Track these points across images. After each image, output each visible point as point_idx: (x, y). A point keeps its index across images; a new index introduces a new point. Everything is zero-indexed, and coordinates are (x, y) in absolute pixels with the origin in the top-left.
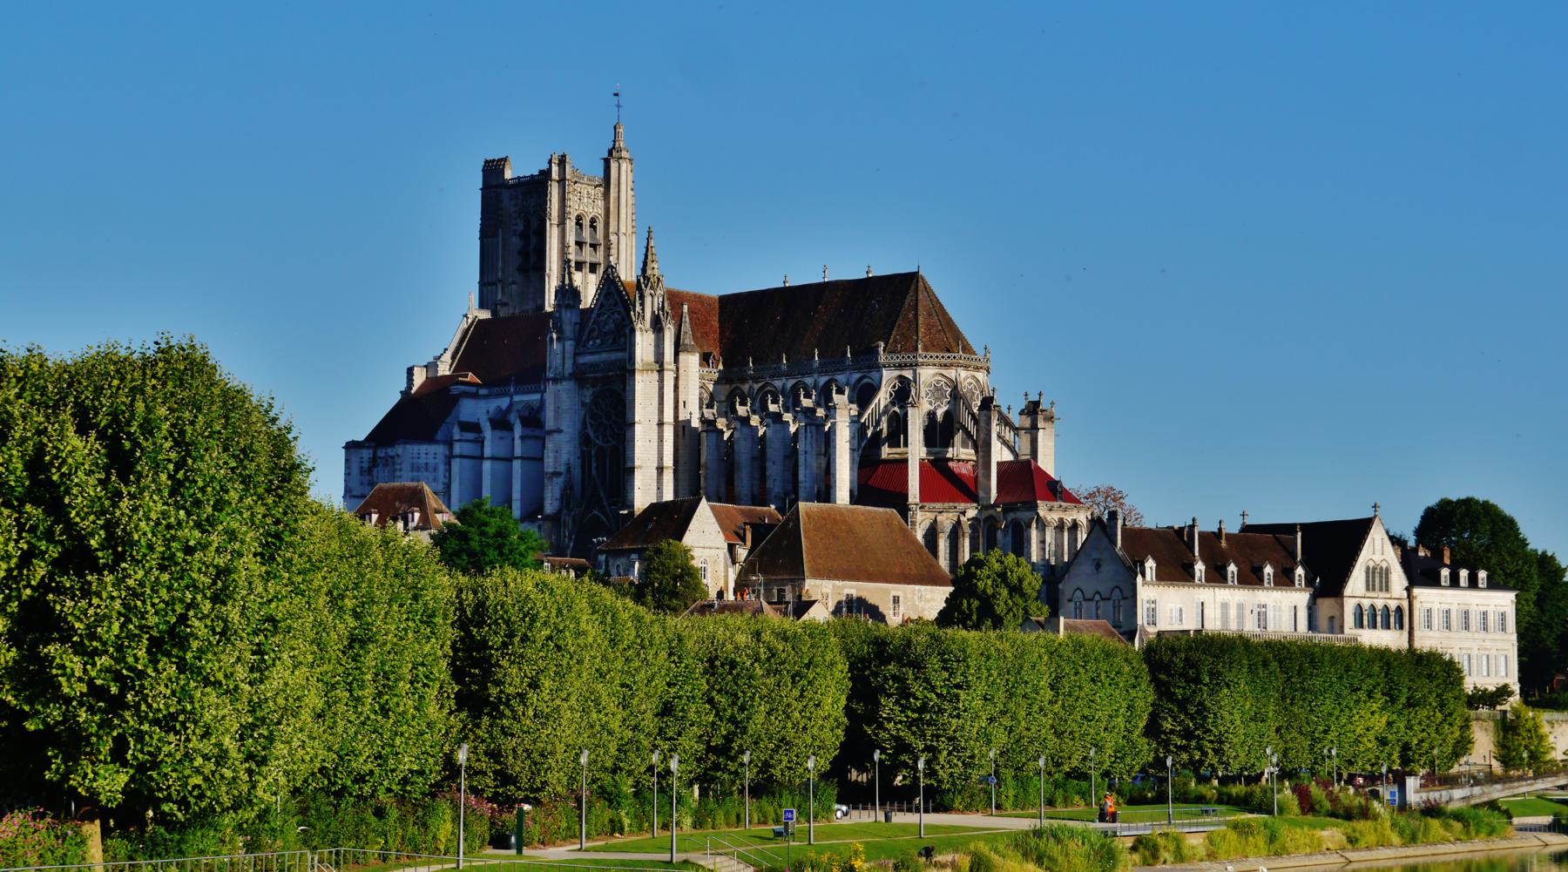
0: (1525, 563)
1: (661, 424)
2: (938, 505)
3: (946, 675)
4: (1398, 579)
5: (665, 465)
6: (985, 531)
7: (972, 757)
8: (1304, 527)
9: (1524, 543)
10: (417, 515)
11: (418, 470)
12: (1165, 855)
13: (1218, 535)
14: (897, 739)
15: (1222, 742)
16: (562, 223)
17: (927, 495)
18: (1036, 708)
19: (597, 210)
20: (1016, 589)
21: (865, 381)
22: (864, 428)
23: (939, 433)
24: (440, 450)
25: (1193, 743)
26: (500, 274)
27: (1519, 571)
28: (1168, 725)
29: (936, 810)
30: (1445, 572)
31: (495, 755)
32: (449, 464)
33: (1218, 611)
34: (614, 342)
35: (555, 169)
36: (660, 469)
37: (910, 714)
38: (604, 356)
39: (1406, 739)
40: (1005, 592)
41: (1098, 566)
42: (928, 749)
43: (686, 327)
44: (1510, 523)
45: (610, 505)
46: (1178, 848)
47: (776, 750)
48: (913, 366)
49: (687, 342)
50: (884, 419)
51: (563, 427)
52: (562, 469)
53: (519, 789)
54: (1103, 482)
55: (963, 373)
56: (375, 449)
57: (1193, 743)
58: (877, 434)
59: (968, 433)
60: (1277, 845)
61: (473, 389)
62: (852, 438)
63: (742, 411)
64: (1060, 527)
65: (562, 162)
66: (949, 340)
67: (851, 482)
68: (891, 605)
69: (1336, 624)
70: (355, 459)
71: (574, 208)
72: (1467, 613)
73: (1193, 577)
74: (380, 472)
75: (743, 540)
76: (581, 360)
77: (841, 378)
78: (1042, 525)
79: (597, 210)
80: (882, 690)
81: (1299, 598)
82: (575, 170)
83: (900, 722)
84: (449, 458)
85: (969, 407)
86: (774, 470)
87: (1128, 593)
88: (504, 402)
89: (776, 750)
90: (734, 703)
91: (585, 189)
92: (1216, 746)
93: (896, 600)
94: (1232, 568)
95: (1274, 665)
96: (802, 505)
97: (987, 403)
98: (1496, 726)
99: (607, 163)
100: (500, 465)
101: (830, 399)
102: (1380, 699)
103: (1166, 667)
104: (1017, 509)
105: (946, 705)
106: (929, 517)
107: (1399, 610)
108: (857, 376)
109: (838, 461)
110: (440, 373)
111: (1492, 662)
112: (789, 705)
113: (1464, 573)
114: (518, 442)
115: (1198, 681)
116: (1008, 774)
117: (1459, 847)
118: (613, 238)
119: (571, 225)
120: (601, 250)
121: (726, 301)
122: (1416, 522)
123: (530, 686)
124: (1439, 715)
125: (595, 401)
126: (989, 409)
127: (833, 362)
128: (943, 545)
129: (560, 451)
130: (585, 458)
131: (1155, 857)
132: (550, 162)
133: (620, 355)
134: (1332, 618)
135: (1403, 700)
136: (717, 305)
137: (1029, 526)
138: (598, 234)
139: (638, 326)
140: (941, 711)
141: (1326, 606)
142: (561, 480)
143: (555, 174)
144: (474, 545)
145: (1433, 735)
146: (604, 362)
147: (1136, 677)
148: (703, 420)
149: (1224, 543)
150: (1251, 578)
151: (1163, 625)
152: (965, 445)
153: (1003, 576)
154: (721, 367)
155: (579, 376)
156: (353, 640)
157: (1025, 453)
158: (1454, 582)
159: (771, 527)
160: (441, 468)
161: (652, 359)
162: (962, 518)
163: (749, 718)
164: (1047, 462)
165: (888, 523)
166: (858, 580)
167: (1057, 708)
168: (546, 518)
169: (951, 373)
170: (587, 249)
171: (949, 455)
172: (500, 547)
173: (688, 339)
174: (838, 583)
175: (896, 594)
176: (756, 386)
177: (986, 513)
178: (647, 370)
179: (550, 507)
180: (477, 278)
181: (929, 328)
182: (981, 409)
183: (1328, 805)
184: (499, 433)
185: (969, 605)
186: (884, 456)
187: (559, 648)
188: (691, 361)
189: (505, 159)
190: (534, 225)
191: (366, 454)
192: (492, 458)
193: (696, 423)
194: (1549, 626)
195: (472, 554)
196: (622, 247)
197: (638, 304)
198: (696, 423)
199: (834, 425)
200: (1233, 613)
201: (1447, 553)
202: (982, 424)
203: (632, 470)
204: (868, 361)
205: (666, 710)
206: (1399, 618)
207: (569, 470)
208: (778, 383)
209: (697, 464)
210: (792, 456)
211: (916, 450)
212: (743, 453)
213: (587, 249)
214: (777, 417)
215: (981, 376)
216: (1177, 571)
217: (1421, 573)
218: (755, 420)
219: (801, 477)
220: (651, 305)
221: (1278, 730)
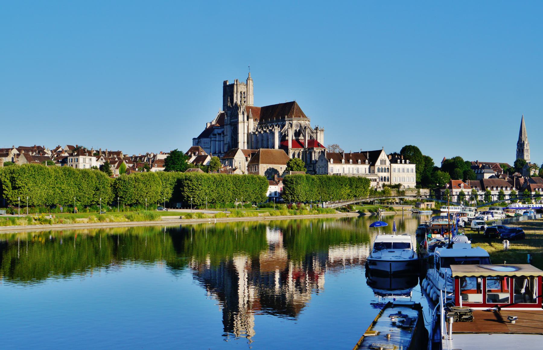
0: (421, 158)
1: (244, 133)
2: (295, 149)
3: (197, 183)
4: (388, 162)
5: (245, 141)
8: (369, 152)
10: (197, 153)
11: (205, 143)
13: (350, 154)
14: (187, 195)
15: (298, 196)
16: (237, 93)
17: (293, 146)
22: (282, 133)
23: (297, 134)
24: (209, 139)
28: (287, 192)
30: (399, 161)
33: (348, 170)
35: (235, 82)
36: (244, 142)
39: (355, 194)
40: (296, 166)
41: (322, 160)
42: (193, 197)
43: (251, 113)
47: (140, 197)
51: (228, 134)
52: (228, 143)
54: (335, 143)
55: (302, 122)
58: (285, 135)
62: (279, 135)
63: (259, 130)
65: (237, 81)
66: (300, 114)
67: (279, 144)
68: (280, 169)
69: (374, 172)
70: (194, 141)
72: (404, 169)
73: (342, 162)
75: (250, 156)
76: (232, 121)
77: (279, 123)
78: (315, 152)
79: (245, 90)
81: (367, 166)
85: (302, 129)
86: (265, 142)
87: (327, 166)
89: (140, 197)
93: (281, 168)
94: (351, 161)
98: (397, 192)
99: (247, 80)
100: (219, 142)
103: (287, 181)
106: (294, 151)
107: (388, 168)
108: (282, 123)
109: (275, 140)
110: (213, 124)
111: (410, 179)
113: (403, 161)
114: (222, 137)
115: (293, 183)
117: (313, 215)
118: (248, 96)
120: (246, 98)
125: (233, 129)
127: (278, 120)
129: (228, 139)
130: (232, 140)
133: (235, 120)
134: (373, 170)
138: (244, 95)
139: (239, 114)
140: (196, 190)
141: (372, 167)
142: (227, 145)
143: (235, 84)
144: (173, 158)
145: (362, 194)
149: (351, 155)
150: (355, 162)
151: (335, 172)
155: (231, 124)
158: (401, 162)
160: (209, 143)
161: (242, 120)
164: (321, 139)
165: (281, 152)
169: (300, 122)
172: (178, 159)
177: (305, 150)
178: (241, 122)
181: (296, 112)
184: (219, 136)
188: (251, 121)
191: (197, 140)
192: (218, 141)
195: (173, 160)
196: (250, 97)
197: (239, 109)
200: (351, 169)
201: (402, 157)
202: (305, 131)
206: (388, 170)
211: (290, 137)
212: (260, 139)
215: (307, 122)
218: (262, 132)
219: (269, 143)
220: (242, 109)
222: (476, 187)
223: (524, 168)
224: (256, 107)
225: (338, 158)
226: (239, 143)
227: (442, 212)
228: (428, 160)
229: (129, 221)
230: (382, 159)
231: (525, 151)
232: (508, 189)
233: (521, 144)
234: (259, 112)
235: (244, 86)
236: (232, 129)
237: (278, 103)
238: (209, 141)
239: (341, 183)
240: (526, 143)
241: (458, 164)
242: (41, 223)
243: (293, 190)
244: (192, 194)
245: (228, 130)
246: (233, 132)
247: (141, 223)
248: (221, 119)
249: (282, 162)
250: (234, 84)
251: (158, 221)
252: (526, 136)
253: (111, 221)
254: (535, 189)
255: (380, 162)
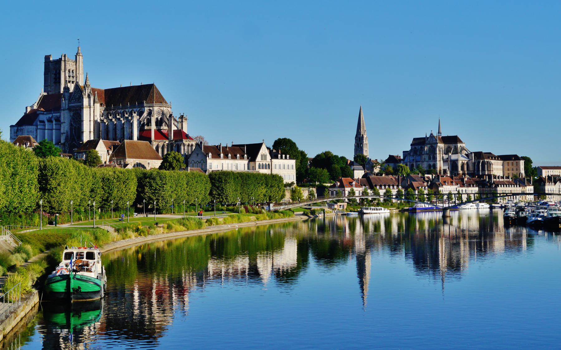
1: (90, 121)
2: (159, 140)
3: (161, 181)
4: (269, 157)
6: (170, 147)
7: (167, 201)
8: (247, 145)
9: (297, 148)
10: (29, 143)
11: (29, 132)
12: (214, 223)
13: (226, 147)
14: (149, 197)
16: (65, 71)
17: (156, 138)
18: (183, 189)
19: (73, 68)
20: (178, 161)
21: (141, 110)
22: (140, 122)
23: (159, 123)
24: (34, 127)
25: (220, 197)
26: (49, 84)
27: (296, 155)
28: (214, 193)
29: (159, 214)
30: (279, 156)
31: (49, 202)
32: (37, 131)
33: (226, 165)
34: (78, 100)
35: (63, 58)
36: (90, 132)
37: (152, 191)
38: (76, 104)
39: (270, 195)
40: (175, 161)
42: (156, 199)
43: (96, 97)
44: (294, 144)
45: (78, 141)
46: (217, 221)
47: (119, 200)
48: (153, 107)
49: (97, 101)
50: (146, 120)
51: (65, 122)
52: (65, 132)
53: (55, 210)
54: (199, 135)
55: (165, 108)
56: (18, 127)
57: (220, 197)
58: (144, 123)
59: (166, 123)
60: (240, 220)
61: (42, 112)
62: (138, 124)
63: (110, 118)
64: (189, 145)
65: (65, 56)
66: (161, 100)
69: (254, 168)
70: (13, 130)
71: (68, 67)
74: (19, 133)
75: (111, 149)
76: (70, 105)
77: (135, 109)
78: (184, 145)
79: (74, 68)
80: (146, 186)
81: (246, 162)
82: (68, 58)
83: (150, 193)
84: (37, 130)
85: (166, 117)
88: (50, 116)
89: (119, 200)
90: (109, 189)
91: (70, 63)
92: (226, 197)
93: (149, 163)
94: (230, 155)
95: (240, 178)
96: (125, 141)
97: (171, 116)
98: (291, 191)
99: (76, 56)
100: (50, 131)
101: (132, 115)
102: (265, 186)
103: (214, 179)
104: (178, 141)
105: (161, 189)
106: (157, 143)
108: (139, 109)
109: (134, 130)
111: (290, 176)
112: (122, 189)
113: (284, 156)
114: (54, 125)
115: (221, 182)
116: (176, 205)
117: (282, 220)
119: (67, 72)
120: (75, 78)
121: (106, 90)
122: (273, 144)
123: (58, 185)
124: (278, 189)
125: (73, 115)
126: (171, 117)
127: (133, 106)
128: (160, 150)
129: (65, 128)
130: (71, 129)
131: (211, 224)
132: (62, 56)
135: (270, 186)
136: (104, 92)
137: (181, 145)
138: (74, 74)
139: (84, 97)
140: (160, 190)
141: (252, 164)
142: (65, 134)
144: (43, 151)
146: (76, 106)
147: (207, 181)
148: (101, 120)
149: (228, 149)
150: (234, 157)
152: (165, 126)
153: (175, 157)
154: (105, 107)
155: (70, 109)
156: (13, 174)
157: (180, 127)
158: (282, 158)
159: (118, 146)
160: (35, 132)
161: (88, 105)
162: (165, 144)
163: (113, 192)
164: (185, 130)
166: (139, 159)
167: (188, 189)
168: (61, 144)
169: (162, 108)
170: (71, 78)
171: (161, 128)
173: (97, 100)
174: (134, 159)
175: (148, 162)
176: (114, 112)
179: (62, 141)
180: (43, 85)
181: (156, 97)
182: (169, 117)
183: (252, 211)
184: (49, 123)
185: (167, 164)
186: (145, 129)
187: (65, 176)
188: (98, 105)
189: (50, 55)
190: (58, 71)
191: (16, 128)
192: (48, 129)
193: (99, 121)
194: (303, 168)
195: (43, 153)
198: (99, 121)
199: (133, 121)
200: (230, 166)
201: (280, 151)
202: (169, 121)
203: (83, 132)
204: (141, 105)
205: (92, 191)
206: (269, 166)
207: (67, 132)
208: (119, 111)
209: (99, 131)
210: (123, 128)
211: (153, 127)
212: (111, 128)
213: (71, 78)
214: (119, 119)
215: (169, 109)
216: (217, 155)
217: (274, 156)
218: (114, 120)
219: (125, 134)
220: (87, 91)
221: (240, 193)
222: (365, 186)
223: (367, 165)
224: (99, 89)
225: (216, 151)
226: (84, 133)
227: (365, 213)
228: (303, 154)
229: (186, 229)
230: (262, 154)
231: (364, 146)
232: (395, 187)
233: (360, 138)
234: (104, 96)
235: (72, 63)
236: (72, 115)
237: (119, 87)
238: (35, 129)
239: (259, 182)
240: (365, 136)
241: (333, 160)
242: (140, 235)
243: (222, 189)
244: (155, 196)
245: (65, 116)
246: (73, 119)
247: (196, 232)
248: (44, 101)
249: (149, 156)
250: (62, 58)
251: (204, 229)
252: (365, 129)
253: (176, 231)
254: (418, 188)
255: (260, 157)
